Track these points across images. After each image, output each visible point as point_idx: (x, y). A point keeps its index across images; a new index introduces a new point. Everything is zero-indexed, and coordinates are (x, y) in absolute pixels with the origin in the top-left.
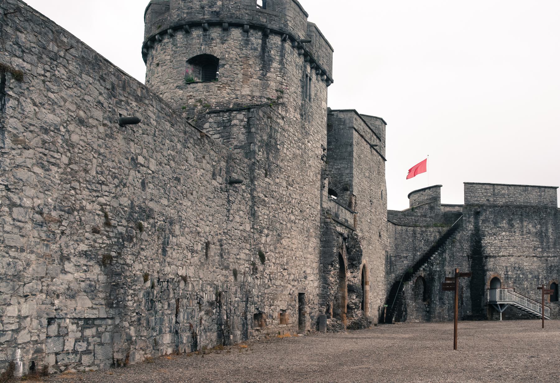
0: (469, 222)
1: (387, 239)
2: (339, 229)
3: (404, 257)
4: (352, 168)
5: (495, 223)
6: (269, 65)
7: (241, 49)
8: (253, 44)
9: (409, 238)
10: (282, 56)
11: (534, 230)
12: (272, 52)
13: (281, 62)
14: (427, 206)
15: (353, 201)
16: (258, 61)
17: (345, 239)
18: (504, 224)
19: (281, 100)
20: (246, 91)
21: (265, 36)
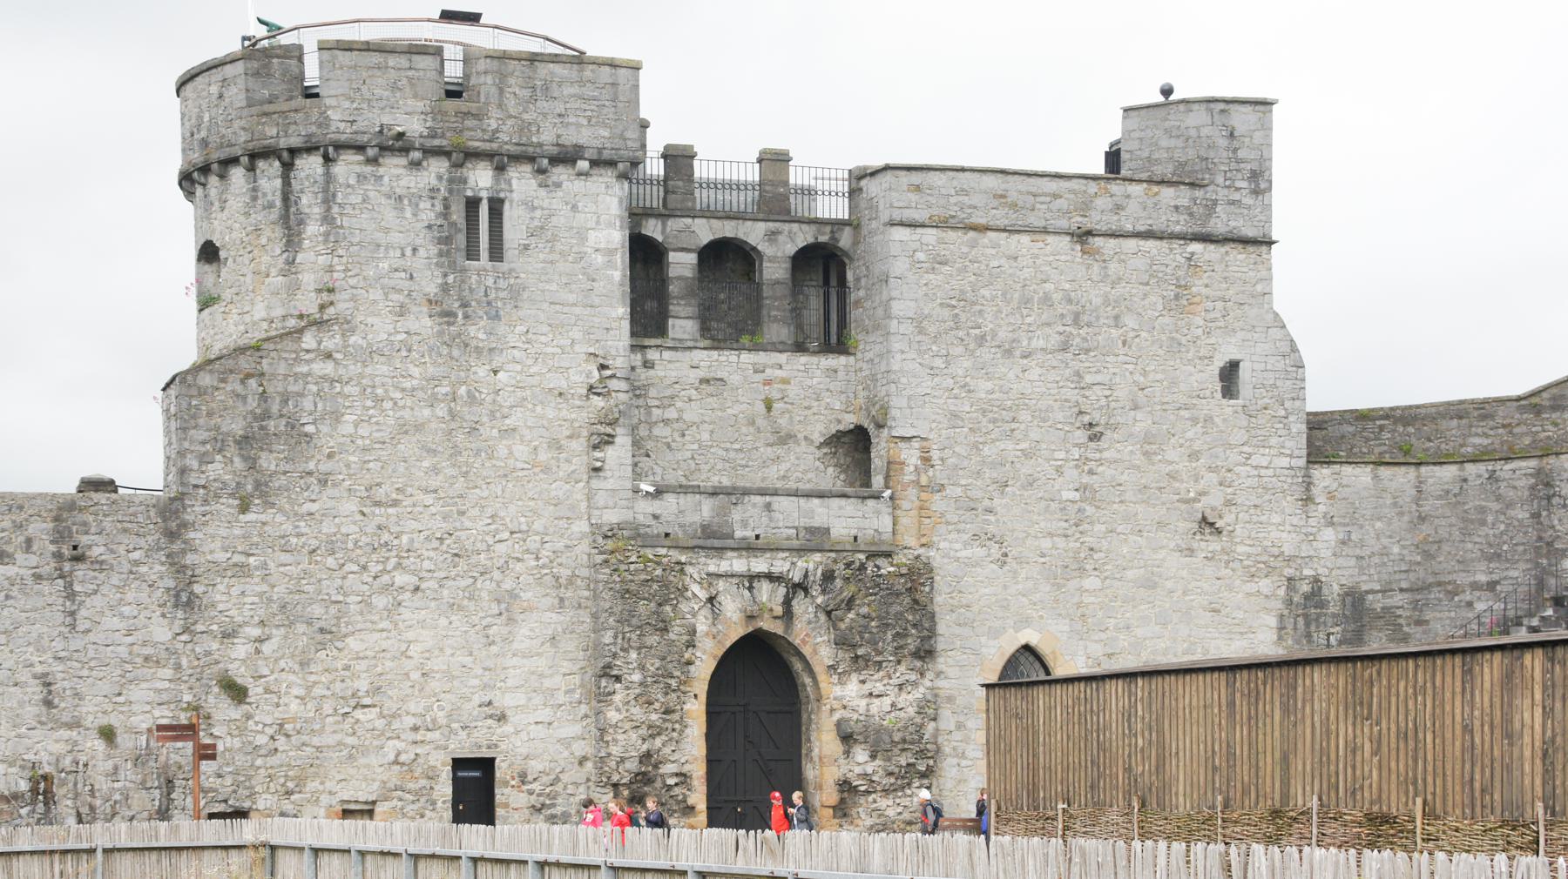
3: (1475, 586)
6: (300, 234)
7: (247, 214)
8: (265, 195)
9: (1510, 505)
10: (328, 199)
12: (304, 201)
13: (327, 219)
16: (279, 232)
19: (331, 311)
20: (259, 312)
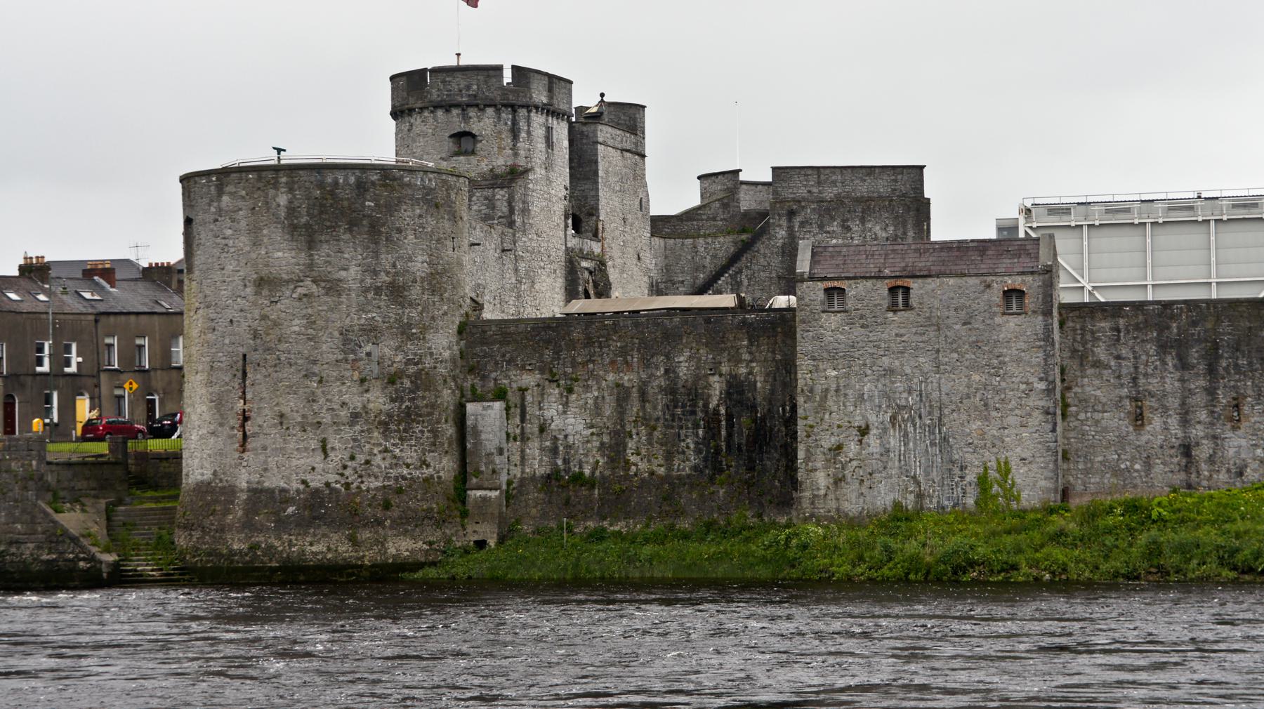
0: (780, 226)
1: (649, 260)
2: (584, 264)
4: (597, 189)
5: (821, 227)
11: (884, 235)
14: (717, 204)
15: (600, 227)
16: (509, 135)
17: (591, 273)
18: (835, 227)
20: (501, 162)
21: (514, 111)
